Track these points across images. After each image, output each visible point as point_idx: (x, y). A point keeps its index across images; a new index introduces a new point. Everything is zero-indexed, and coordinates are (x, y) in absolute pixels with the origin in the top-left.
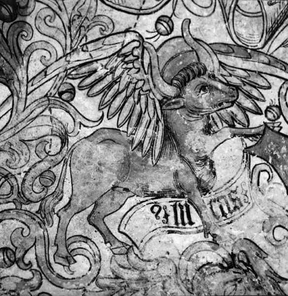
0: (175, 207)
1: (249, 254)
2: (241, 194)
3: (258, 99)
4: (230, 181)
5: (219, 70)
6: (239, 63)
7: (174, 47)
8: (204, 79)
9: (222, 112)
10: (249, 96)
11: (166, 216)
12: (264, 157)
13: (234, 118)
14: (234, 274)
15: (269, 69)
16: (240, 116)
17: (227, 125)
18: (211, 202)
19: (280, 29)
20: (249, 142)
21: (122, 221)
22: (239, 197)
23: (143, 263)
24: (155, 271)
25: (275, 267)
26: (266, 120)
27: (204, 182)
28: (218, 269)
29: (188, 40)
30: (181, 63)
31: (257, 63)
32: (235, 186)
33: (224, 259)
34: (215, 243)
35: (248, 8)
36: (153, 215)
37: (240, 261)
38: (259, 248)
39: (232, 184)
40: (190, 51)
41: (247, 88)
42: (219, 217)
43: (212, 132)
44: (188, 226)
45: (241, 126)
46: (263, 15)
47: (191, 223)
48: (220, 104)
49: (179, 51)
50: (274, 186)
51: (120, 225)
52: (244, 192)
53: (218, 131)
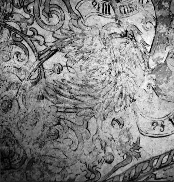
0: (103, 5)
1: (134, 32)
2: (134, 6)
11: (99, 8)
14: (126, 40)
18: (120, 6)
21: (77, 4)
23: (85, 27)
24: (89, 32)
25: (145, 40)
28: (119, 36)
33: (122, 32)
34: (119, 24)
36: (93, 6)
38: (139, 30)
42: (123, 14)
44: (108, 14)
47: (110, 14)
50: (149, 5)
51: (76, 6)
52: (136, 5)
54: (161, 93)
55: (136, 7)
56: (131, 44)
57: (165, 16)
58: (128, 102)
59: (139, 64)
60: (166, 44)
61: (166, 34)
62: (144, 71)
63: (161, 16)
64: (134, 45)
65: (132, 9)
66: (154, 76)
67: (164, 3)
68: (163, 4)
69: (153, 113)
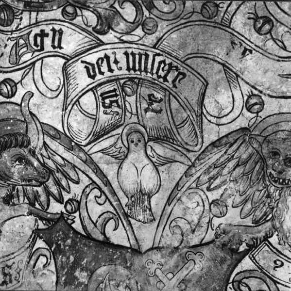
3: (64, 189)
4: (9, 255)
5: (41, 149)
6: (61, 150)
7: (9, 111)
8: (25, 152)
9: (28, 188)
10: (58, 183)
12: (49, 243)
13: (36, 196)
15: (83, 167)
16: (43, 198)
17: (28, 202)
19: (105, 137)
20: (41, 225)
22: (11, 273)
26: (64, 211)
29: (24, 111)
30: (9, 128)
31: (75, 157)
32: (12, 261)
35: (87, 107)
39: (10, 259)
40: (22, 121)
41: (59, 175)
43: (11, 203)
45: (40, 208)
46: (95, 119)
48: (30, 181)
49: (12, 117)
50: (47, 273)
53: (18, 204)
55: (19, 273)
65: (8, 277)
67: (80, 272)
68: (77, 273)
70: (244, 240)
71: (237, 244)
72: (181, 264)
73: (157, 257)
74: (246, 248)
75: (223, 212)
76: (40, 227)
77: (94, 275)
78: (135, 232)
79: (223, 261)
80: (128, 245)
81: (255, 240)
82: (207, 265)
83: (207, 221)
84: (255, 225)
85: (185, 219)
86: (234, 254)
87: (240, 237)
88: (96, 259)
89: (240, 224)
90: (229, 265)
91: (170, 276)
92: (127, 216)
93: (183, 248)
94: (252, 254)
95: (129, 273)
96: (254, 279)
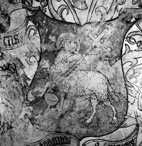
1: (16, 65)
2: (20, 37)
4: (16, 30)
12: (35, 22)
14: (7, 73)
17: (21, 2)
18: (4, 37)
22: (18, 38)
25: (27, 73)
27: (4, 26)
32: (18, 32)
33: (4, 65)
37: (11, 68)
38: (22, 64)
39: (17, 31)
42: (7, 46)
43: (13, 3)
45: (28, 4)
50: (36, 38)
52: (21, 37)
53: (17, 3)
54: (36, 122)
55: (22, 38)
56: (12, 77)
57: (50, 51)
58: (6, 129)
59: (19, 97)
60: (47, 80)
61: (48, 69)
62: (23, 103)
63: (46, 50)
64: (16, 78)
66: (31, 108)
67: (52, 36)
68: (50, 37)
69: (27, 139)
70: (133, 16)
71: (130, 18)
72: (101, 30)
73: (89, 27)
74: (135, 20)
75: (123, 1)
76: (29, 15)
77: (58, 38)
78: (78, 15)
79: (122, 27)
80: (74, 22)
81: (139, 16)
82: (114, 30)
83: (115, 7)
84: (139, 8)
85: (103, 7)
86: (128, 24)
87: (131, 14)
88: (58, 30)
89: (132, 8)
90: (125, 30)
91: (96, 36)
92: (73, 7)
93: (102, 22)
94: (138, 23)
95: (75, 36)
96: (137, 35)
